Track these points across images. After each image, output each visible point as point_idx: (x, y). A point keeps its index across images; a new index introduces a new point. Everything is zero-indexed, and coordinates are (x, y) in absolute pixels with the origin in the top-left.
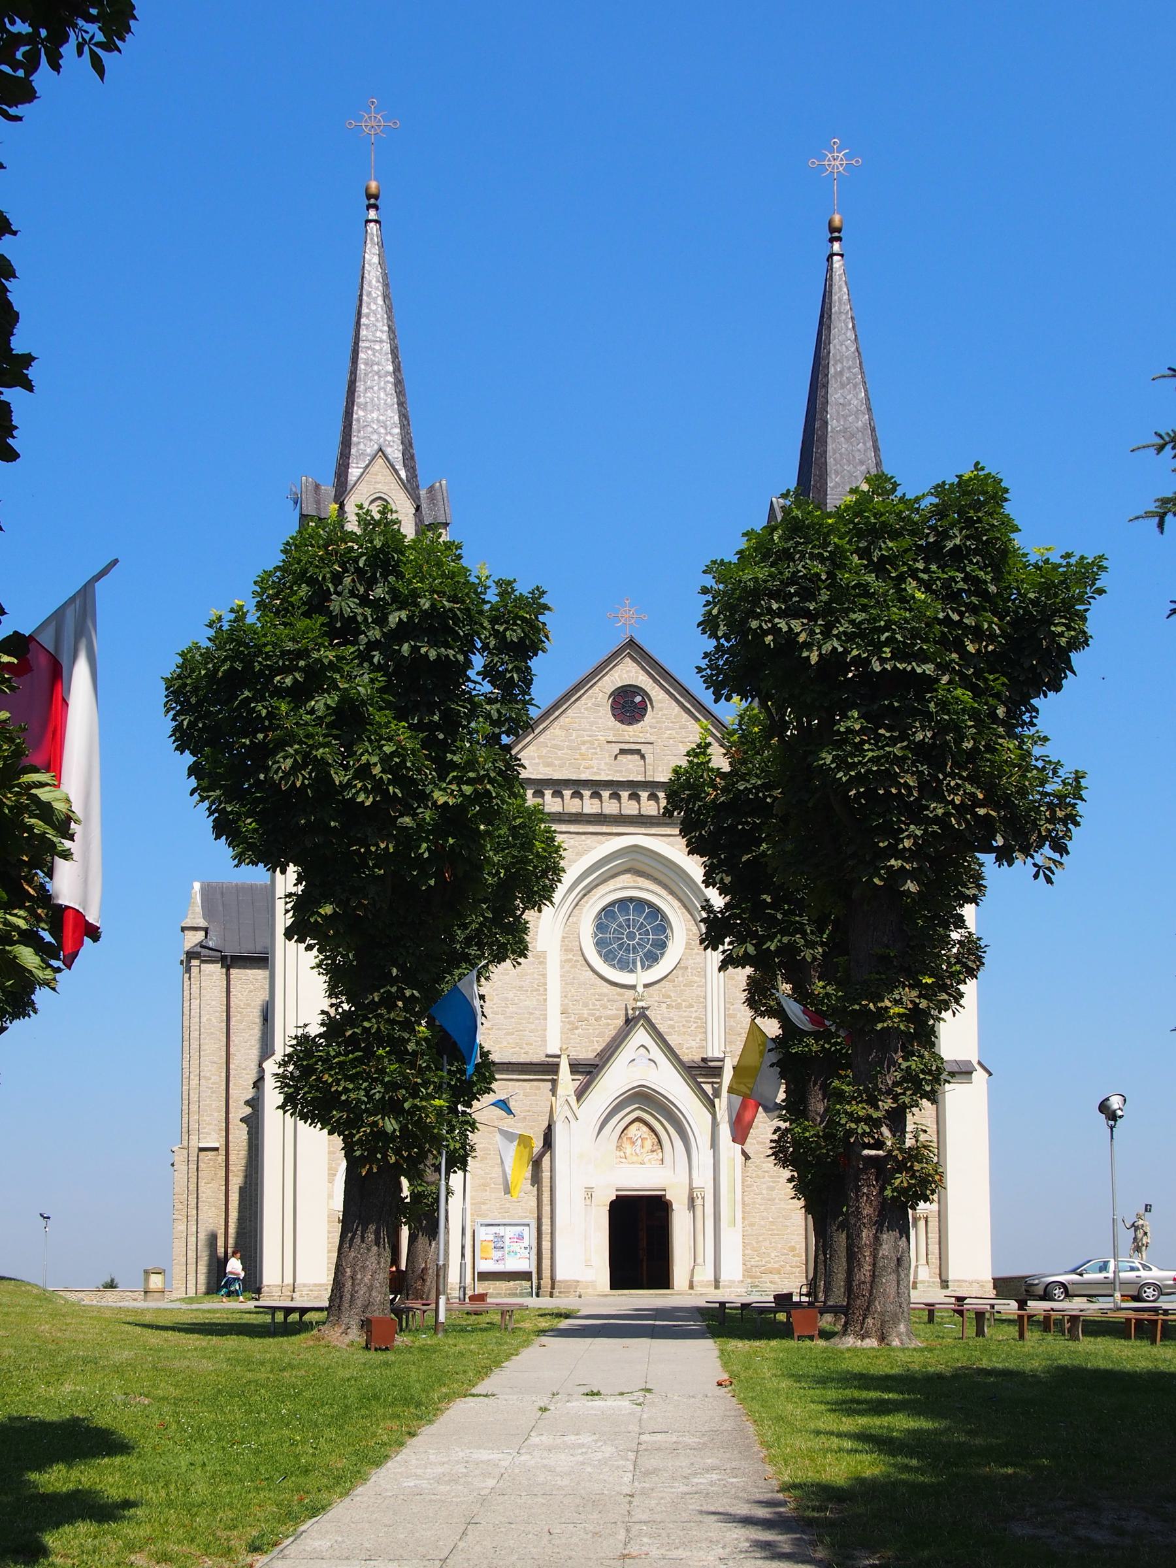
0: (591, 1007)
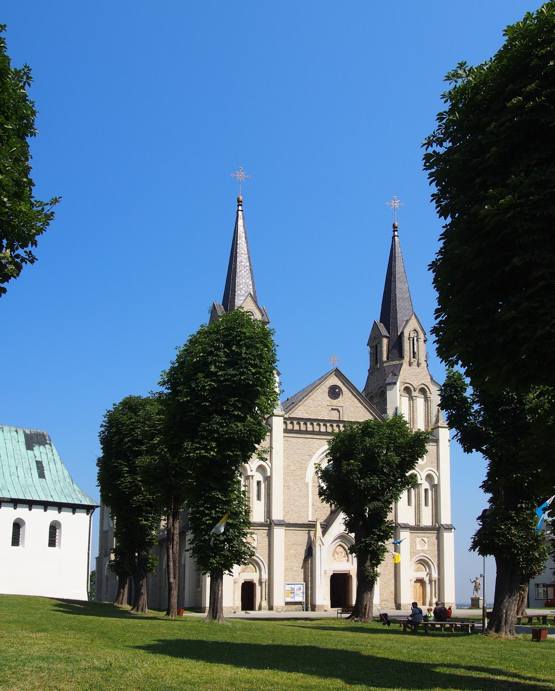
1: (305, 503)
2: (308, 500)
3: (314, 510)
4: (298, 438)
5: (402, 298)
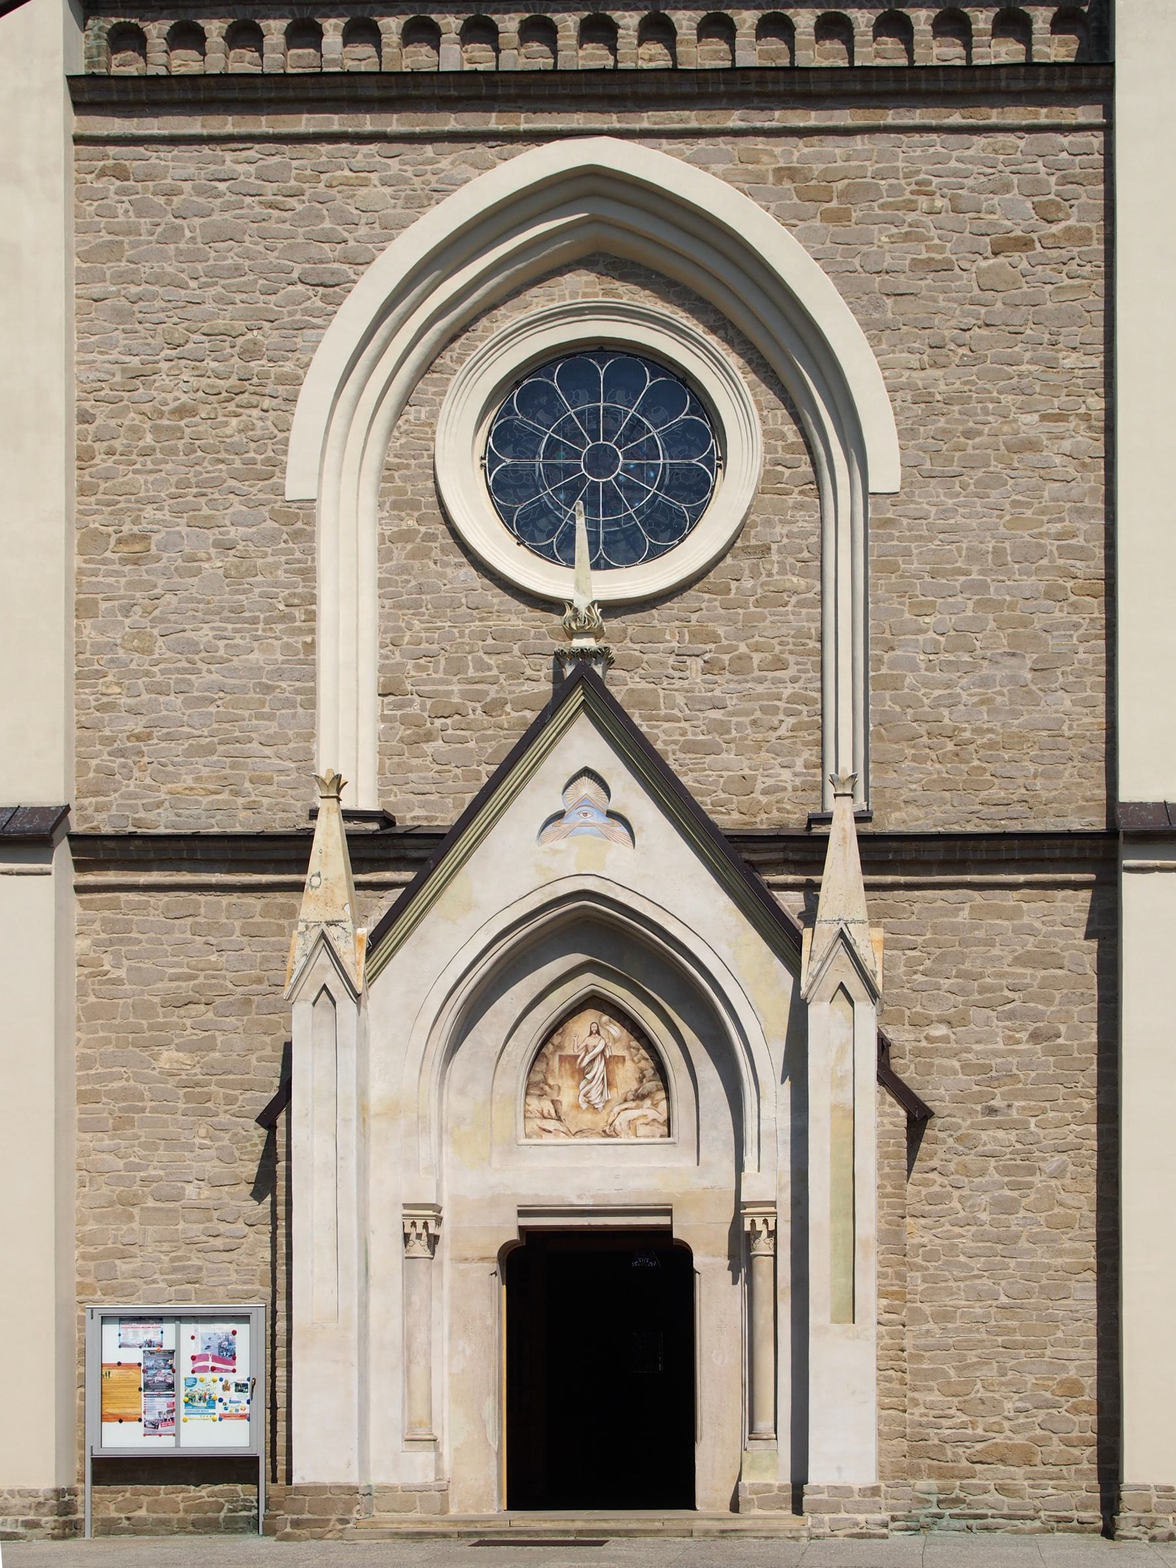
0: (471, 672)
1: (281, 675)
2: (311, 647)
3: (403, 732)
4: (218, 150)
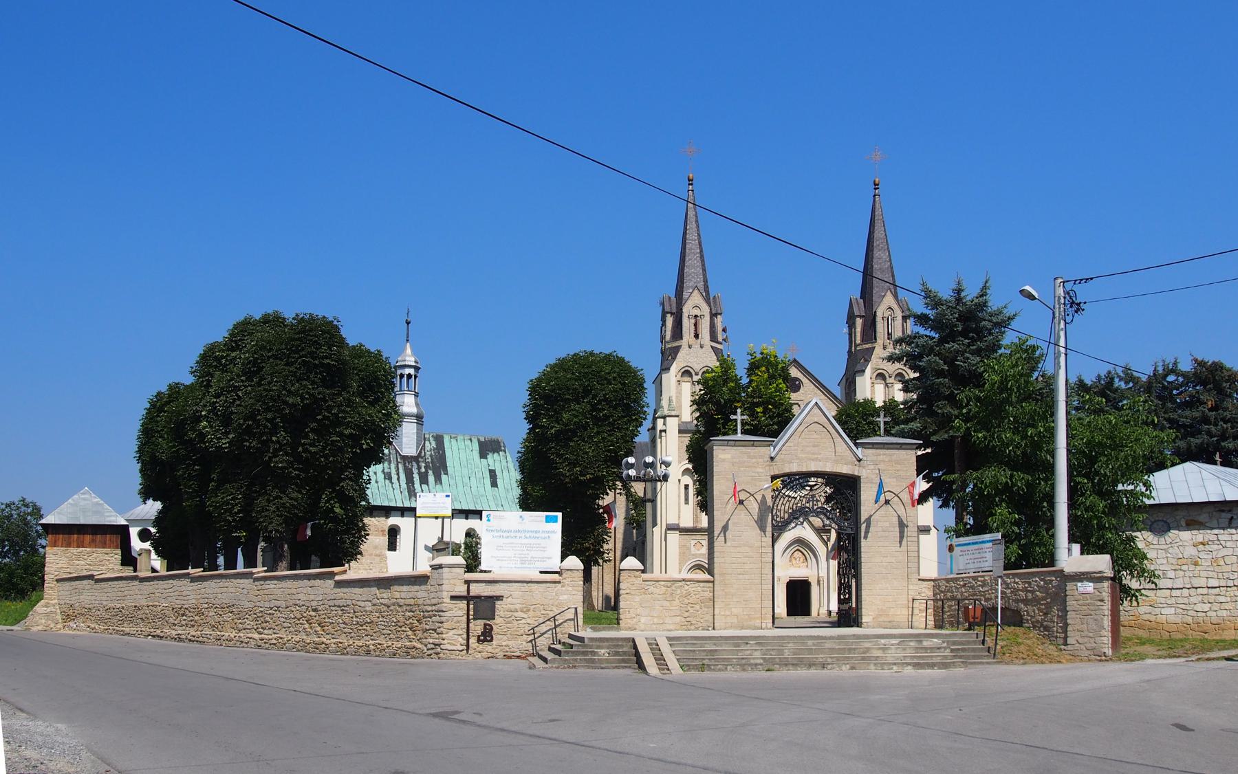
5: (880, 269)
